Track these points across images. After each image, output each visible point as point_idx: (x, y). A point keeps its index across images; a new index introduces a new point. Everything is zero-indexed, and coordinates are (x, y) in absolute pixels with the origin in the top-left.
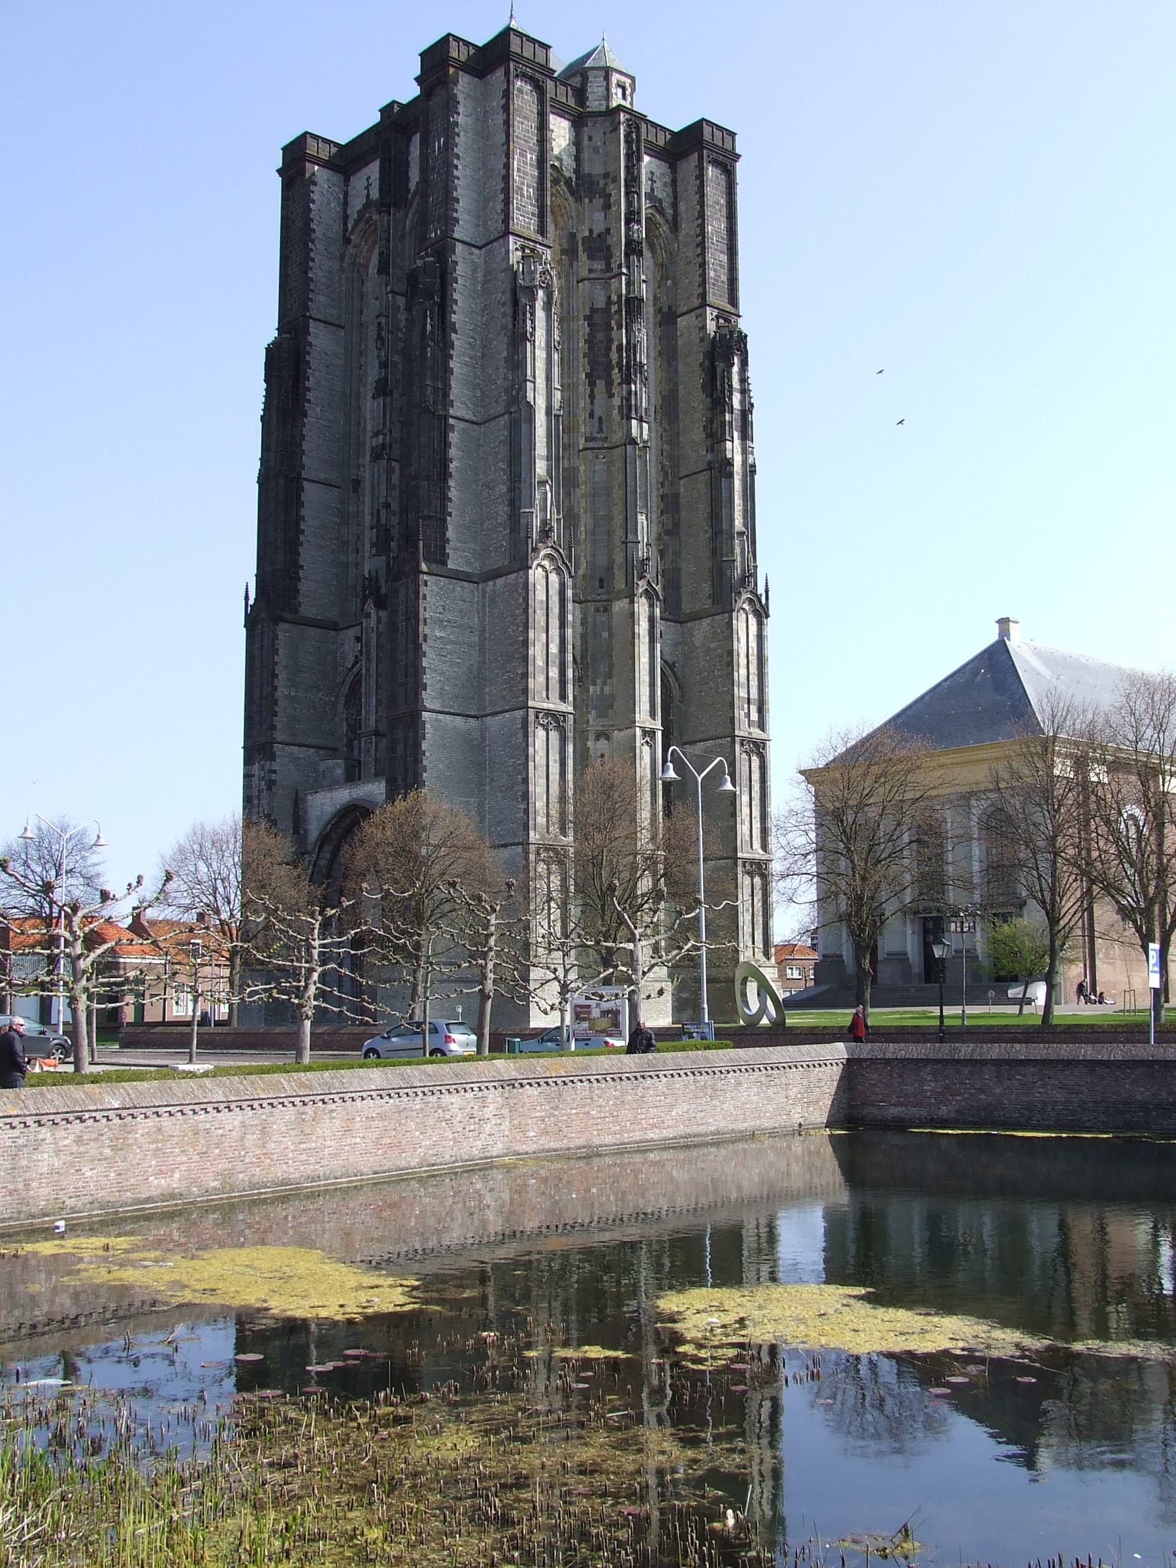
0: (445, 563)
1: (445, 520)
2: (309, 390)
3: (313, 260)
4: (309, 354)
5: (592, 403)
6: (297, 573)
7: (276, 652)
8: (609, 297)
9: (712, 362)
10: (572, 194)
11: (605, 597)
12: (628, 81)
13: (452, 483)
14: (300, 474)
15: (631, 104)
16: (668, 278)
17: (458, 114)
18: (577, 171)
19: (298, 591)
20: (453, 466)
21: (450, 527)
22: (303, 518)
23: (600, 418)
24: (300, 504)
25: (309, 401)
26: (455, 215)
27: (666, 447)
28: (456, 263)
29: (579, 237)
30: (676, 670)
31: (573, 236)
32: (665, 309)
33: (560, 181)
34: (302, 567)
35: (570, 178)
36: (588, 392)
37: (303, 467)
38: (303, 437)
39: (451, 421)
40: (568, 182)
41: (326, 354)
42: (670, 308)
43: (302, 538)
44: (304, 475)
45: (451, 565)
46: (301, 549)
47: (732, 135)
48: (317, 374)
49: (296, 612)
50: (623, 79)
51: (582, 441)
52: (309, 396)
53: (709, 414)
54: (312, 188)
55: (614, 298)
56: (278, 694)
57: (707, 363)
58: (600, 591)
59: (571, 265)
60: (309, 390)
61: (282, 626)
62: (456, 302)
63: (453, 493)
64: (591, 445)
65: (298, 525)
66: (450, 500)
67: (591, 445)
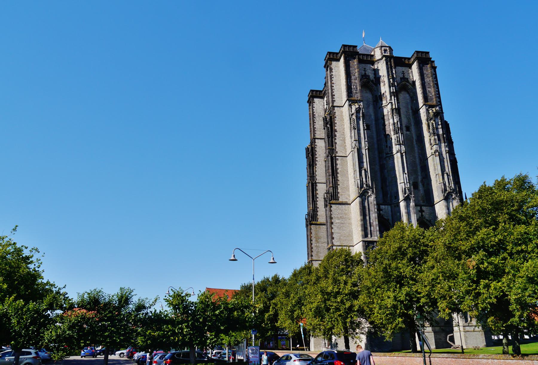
0: (338, 200)
1: (337, 187)
2: (317, 158)
3: (315, 123)
4: (316, 148)
5: (387, 143)
6: (317, 210)
7: (311, 233)
8: (388, 111)
9: (428, 121)
10: (374, 84)
11: (397, 202)
12: (388, 48)
13: (338, 175)
14: (316, 181)
15: (390, 54)
16: (414, 100)
17: (333, 72)
18: (374, 78)
19: (317, 215)
20: (338, 171)
21: (339, 189)
22: (318, 194)
23: (390, 147)
24: (316, 190)
25: (317, 161)
26: (334, 99)
27: (420, 151)
28: (335, 112)
29: (378, 95)
30: (431, 222)
31: (376, 96)
32: (414, 110)
33: (370, 82)
34: (318, 208)
35: (373, 80)
36: (385, 140)
37: (316, 179)
38: (316, 171)
39: (337, 157)
40: (372, 81)
41: (321, 147)
42: (416, 109)
43: (317, 199)
44: (317, 182)
45: (340, 200)
46: (317, 203)
47: (428, 53)
48: (319, 153)
49: (317, 221)
50: (386, 48)
51: (385, 155)
52: (317, 159)
53: (429, 138)
54: (313, 104)
55: (389, 110)
56: (312, 246)
57: (427, 122)
58: (395, 200)
59: (377, 105)
60: (317, 158)
61: (312, 226)
62: (336, 123)
63: (339, 178)
64: (387, 156)
65: (316, 196)
66: (339, 180)
67: (387, 156)
